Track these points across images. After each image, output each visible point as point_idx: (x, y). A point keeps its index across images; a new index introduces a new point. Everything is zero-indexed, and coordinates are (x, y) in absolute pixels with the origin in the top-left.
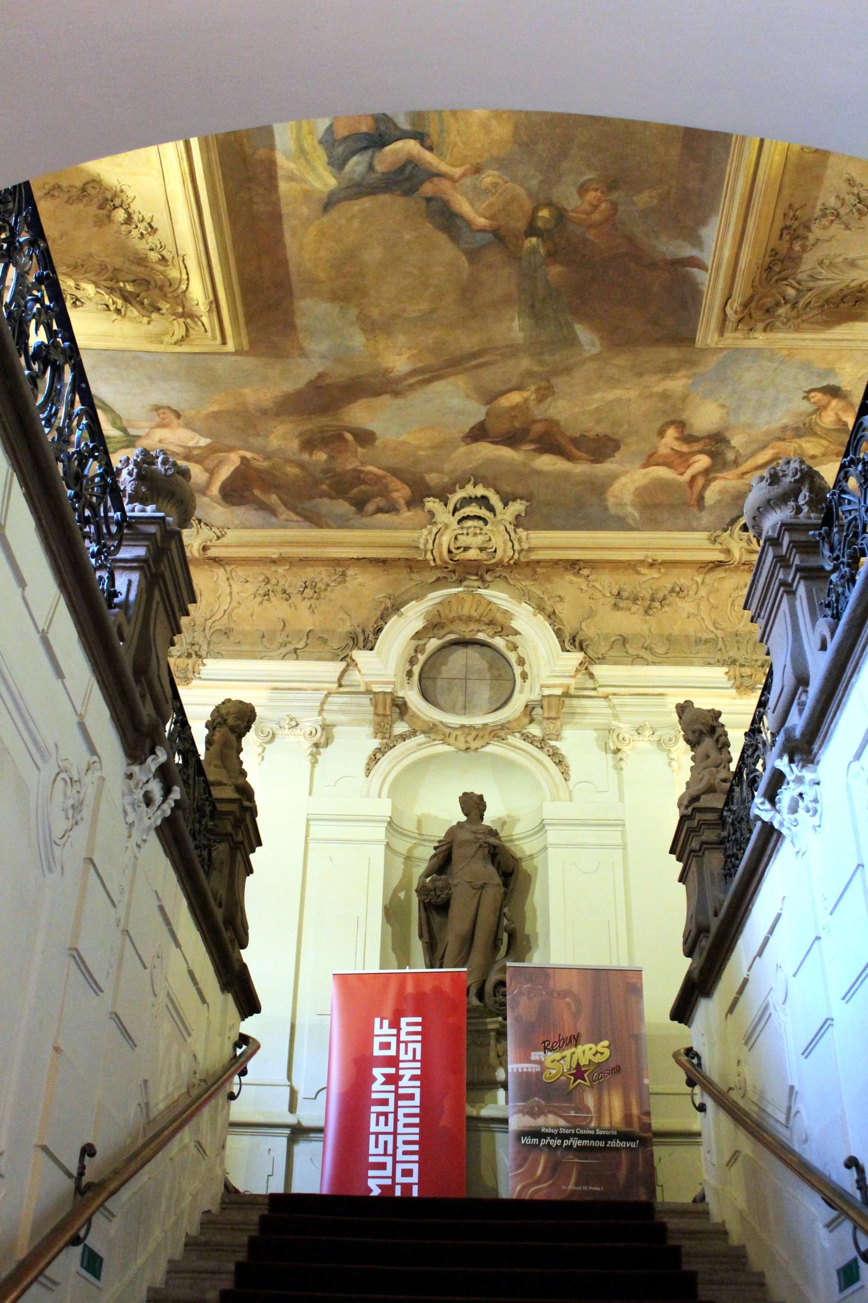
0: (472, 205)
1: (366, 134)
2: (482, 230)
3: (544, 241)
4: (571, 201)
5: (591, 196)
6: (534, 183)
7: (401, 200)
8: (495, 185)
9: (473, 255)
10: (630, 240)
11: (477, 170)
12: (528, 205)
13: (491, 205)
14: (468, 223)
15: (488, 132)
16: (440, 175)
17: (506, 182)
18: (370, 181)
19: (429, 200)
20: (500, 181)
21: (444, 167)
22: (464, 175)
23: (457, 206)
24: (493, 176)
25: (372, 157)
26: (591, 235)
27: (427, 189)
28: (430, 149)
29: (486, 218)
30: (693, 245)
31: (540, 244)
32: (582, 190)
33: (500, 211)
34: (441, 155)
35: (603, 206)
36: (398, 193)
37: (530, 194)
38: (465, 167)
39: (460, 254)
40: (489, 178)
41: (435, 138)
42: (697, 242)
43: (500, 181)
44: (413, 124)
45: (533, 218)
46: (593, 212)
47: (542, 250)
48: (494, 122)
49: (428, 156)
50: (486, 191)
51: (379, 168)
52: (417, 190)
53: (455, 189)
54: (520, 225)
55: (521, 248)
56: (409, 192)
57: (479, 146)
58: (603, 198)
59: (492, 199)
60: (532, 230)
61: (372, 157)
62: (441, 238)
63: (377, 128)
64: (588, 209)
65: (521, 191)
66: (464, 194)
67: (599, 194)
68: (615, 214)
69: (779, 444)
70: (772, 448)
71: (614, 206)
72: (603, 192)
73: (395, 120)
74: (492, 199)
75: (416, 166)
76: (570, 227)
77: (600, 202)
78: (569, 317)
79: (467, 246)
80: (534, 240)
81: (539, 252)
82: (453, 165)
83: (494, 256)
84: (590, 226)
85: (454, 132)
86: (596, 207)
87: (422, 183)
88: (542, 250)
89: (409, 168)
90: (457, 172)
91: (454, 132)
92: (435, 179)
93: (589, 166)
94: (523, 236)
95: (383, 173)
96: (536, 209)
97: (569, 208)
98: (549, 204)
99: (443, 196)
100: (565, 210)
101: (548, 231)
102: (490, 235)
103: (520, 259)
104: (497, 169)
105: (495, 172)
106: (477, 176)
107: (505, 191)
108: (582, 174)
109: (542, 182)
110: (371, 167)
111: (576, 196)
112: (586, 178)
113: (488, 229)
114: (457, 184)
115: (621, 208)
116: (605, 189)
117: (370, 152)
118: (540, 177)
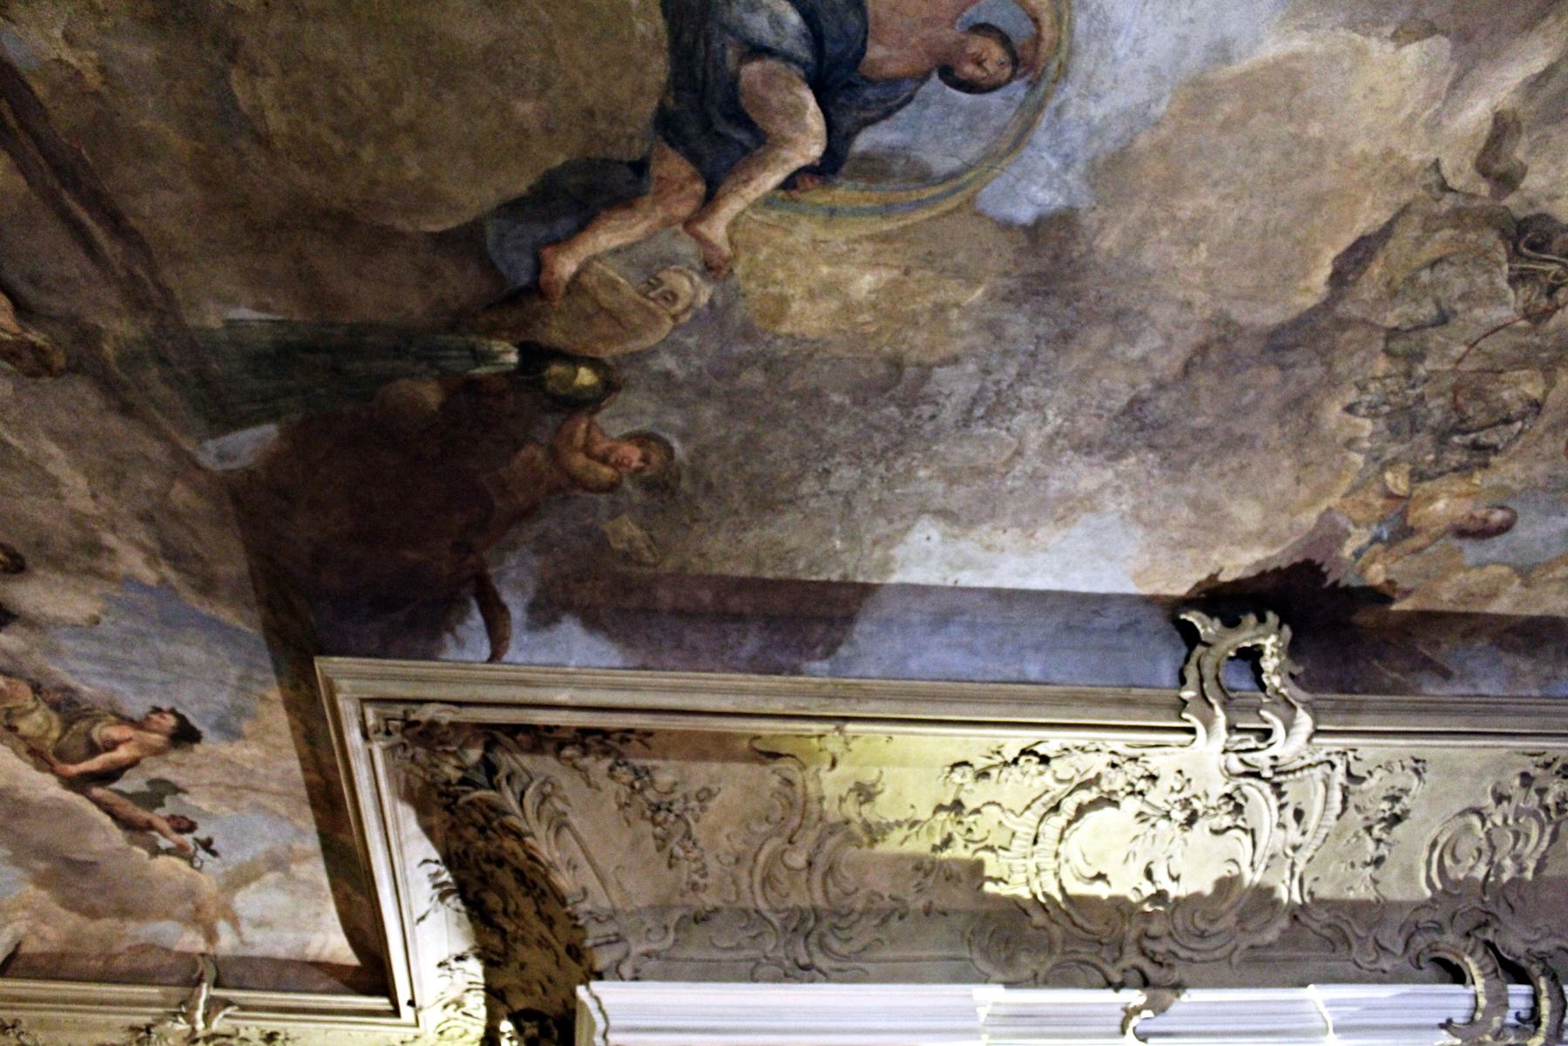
0: (617, 251)
1: (862, 52)
2: (539, 266)
3: (507, 374)
4: (613, 424)
5: (634, 454)
6: (668, 362)
7: (648, 107)
8: (672, 297)
9: (465, 241)
10: (527, 514)
11: (712, 268)
12: (607, 352)
13: (614, 286)
14: (563, 241)
15: (811, 295)
16: (710, 200)
17: (674, 317)
18: (717, 45)
19: (640, 168)
20: (679, 307)
21: (732, 207)
22: (701, 240)
23: (612, 223)
24: (695, 296)
25: (788, 58)
26: (533, 453)
27: (673, 166)
28: (789, 184)
29: (577, 275)
30: (532, 608)
31: (504, 368)
32: (641, 439)
33: (595, 300)
34: (768, 202)
35: (606, 472)
36: (670, 102)
37: (637, 357)
38: (727, 250)
39: (467, 217)
40: (692, 289)
41: (819, 196)
42: (545, 613)
43: (679, 307)
44: (865, 157)
45: (574, 359)
46: (590, 455)
47: (482, 371)
48: (834, 305)
49: (770, 179)
50: (654, 282)
51: (753, 71)
52: (672, 145)
53: (667, 223)
54: (555, 334)
55: (492, 331)
56: (667, 125)
57: (780, 274)
58: (623, 470)
59: (629, 290)
60: (535, 356)
61: (788, 58)
62: (520, 184)
63: (871, 82)
64: (601, 446)
65: (650, 340)
66: (650, 236)
67: (636, 464)
68: (587, 489)
69: (24, 689)
70: (8, 684)
71: (612, 487)
72: (638, 470)
73: (884, 123)
74: (629, 290)
75: (746, 151)
76: (549, 420)
77: (617, 465)
78: (296, 417)
79: (491, 231)
80: (513, 358)
81: (478, 365)
82: (734, 224)
83: (460, 283)
84: (554, 453)
85: (821, 234)
86: (604, 460)
87: (694, 158)
88: (482, 371)
89: (742, 136)
90: (716, 230)
91: (821, 234)
92: (700, 187)
93: (701, 452)
94: (522, 339)
95: (736, 77)
96: (595, 364)
97: (598, 418)
98: (610, 386)
99: (648, 199)
100: (593, 413)
101: (539, 383)
102: (525, 279)
103: (453, 328)
104: (711, 304)
105: (703, 300)
106: (699, 267)
107: (653, 314)
108: (684, 437)
109: (668, 375)
110: (758, 51)
111: (627, 430)
112: (676, 445)
113: (543, 277)
114: (680, 228)
115: (603, 499)
116: (648, 473)
117: (805, 54)
118: (680, 374)
